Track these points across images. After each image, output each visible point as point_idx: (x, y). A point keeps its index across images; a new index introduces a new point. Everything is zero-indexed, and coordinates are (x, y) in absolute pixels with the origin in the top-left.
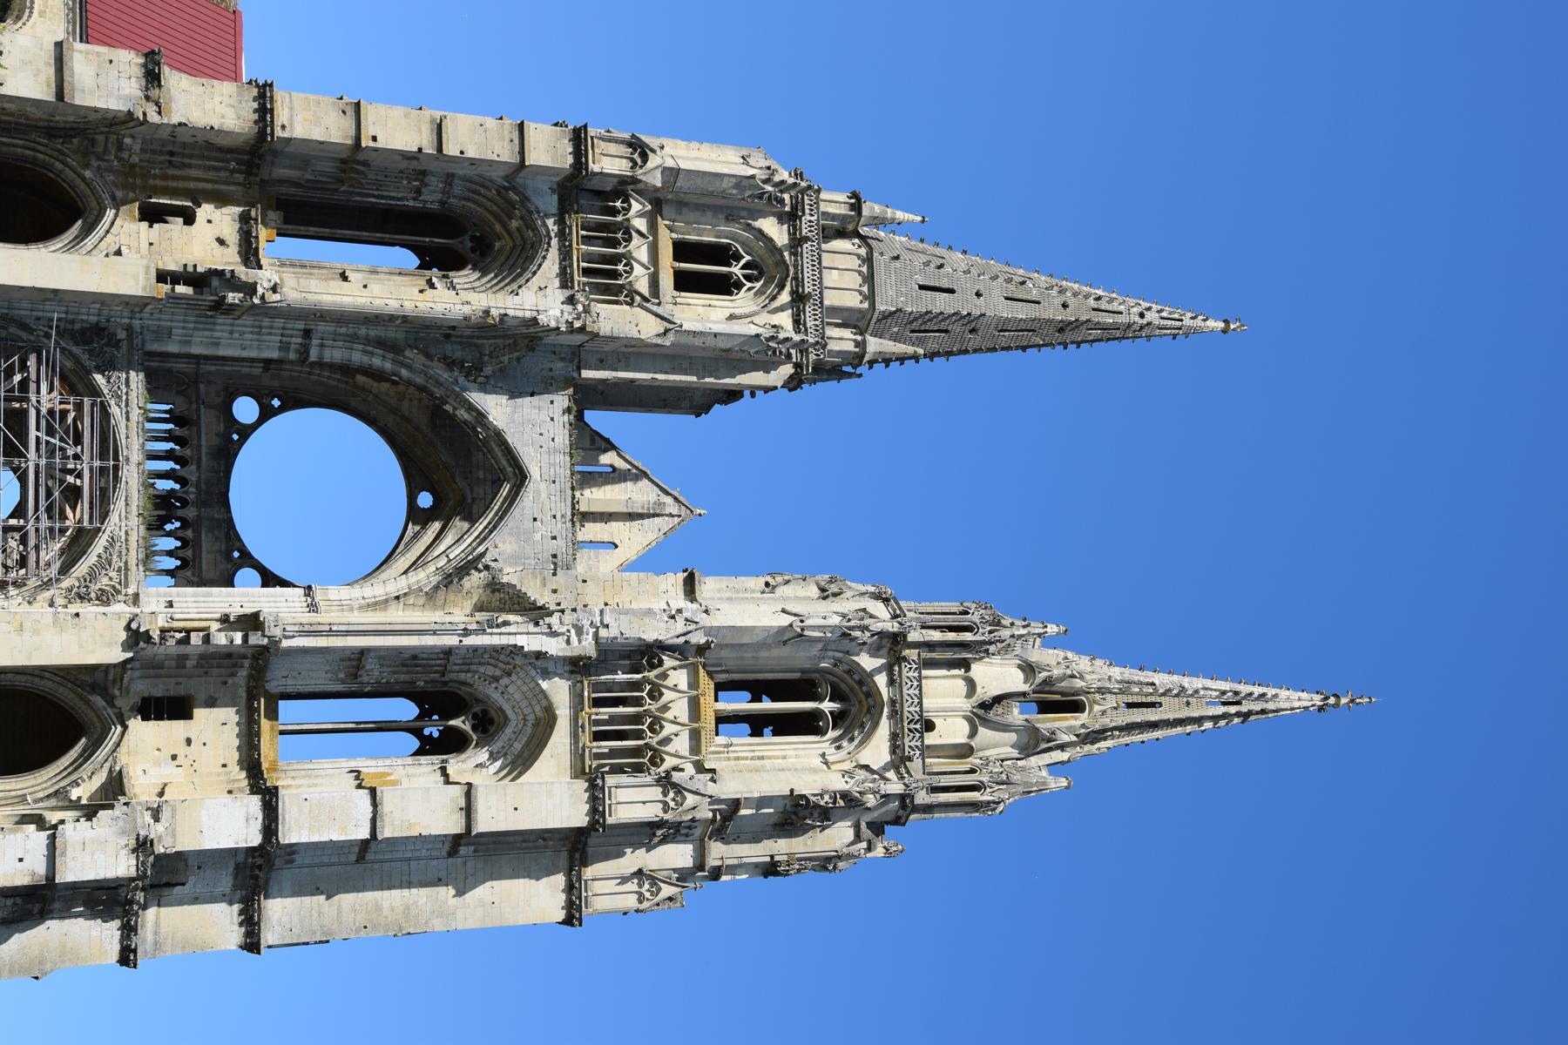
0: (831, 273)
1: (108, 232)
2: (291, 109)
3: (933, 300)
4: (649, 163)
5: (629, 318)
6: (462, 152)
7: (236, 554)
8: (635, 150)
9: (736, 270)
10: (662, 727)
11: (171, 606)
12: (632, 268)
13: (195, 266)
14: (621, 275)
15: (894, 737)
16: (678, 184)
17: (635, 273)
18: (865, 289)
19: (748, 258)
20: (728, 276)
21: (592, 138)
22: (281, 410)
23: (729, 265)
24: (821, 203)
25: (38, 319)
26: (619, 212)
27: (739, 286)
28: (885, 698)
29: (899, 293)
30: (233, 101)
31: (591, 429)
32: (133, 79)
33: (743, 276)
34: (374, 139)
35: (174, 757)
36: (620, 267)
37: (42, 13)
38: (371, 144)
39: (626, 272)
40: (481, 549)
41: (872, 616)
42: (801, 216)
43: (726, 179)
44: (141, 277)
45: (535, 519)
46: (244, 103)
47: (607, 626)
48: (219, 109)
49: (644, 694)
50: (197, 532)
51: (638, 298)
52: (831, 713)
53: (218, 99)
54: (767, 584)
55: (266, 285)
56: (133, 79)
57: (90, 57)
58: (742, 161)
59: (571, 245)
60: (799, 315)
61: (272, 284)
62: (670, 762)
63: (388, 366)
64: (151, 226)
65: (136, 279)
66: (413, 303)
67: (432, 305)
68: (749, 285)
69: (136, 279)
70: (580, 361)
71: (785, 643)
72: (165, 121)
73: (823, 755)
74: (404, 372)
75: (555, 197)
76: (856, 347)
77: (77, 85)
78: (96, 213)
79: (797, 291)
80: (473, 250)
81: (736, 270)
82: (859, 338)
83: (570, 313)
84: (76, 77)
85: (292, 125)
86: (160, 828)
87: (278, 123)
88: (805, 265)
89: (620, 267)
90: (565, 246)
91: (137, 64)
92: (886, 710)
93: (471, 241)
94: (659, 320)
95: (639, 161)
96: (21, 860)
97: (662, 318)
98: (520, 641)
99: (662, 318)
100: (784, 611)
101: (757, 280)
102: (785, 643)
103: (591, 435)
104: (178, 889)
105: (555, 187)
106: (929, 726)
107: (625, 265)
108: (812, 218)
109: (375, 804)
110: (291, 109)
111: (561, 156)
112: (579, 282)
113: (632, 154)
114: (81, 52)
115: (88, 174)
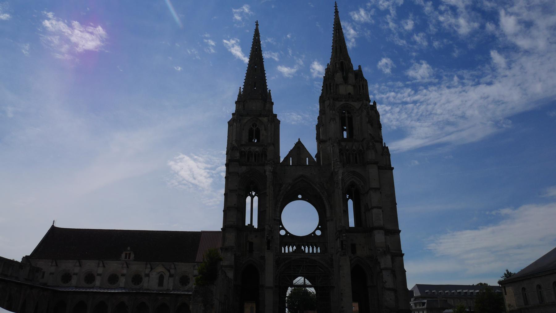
7: (313, 235)
9: (254, 129)
10: (354, 149)
11: (333, 248)
15: (353, 101)
22: (282, 225)
25: (275, 273)
27: (258, 128)
28: (345, 102)
34: (235, 204)
35: (363, 247)
36: (257, 153)
40: (318, 185)
41: (330, 104)
45: (311, 174)
47: (336, 159)
49: (347, 153)
51: (264, 150)
52: (348, 114)
54: (322, 126)
58: (231, 126)
62: (361, 148)
63: (280, 203)
71: (336, 123)
73: (357, 116)
74: (281, 200)
75: (243, 167)
81: (254, 129)
82: (268, 103)
86: (381, 250)
89: (257, 153)
92: (347, 102)
96: (388, 276)
98: (340, 177)
100: (329, 123)
102: (336, 123)
104: (389, 246)
106: (349, 94)
107: (256, 152)
109: (375, 207)
115: (244, 263)
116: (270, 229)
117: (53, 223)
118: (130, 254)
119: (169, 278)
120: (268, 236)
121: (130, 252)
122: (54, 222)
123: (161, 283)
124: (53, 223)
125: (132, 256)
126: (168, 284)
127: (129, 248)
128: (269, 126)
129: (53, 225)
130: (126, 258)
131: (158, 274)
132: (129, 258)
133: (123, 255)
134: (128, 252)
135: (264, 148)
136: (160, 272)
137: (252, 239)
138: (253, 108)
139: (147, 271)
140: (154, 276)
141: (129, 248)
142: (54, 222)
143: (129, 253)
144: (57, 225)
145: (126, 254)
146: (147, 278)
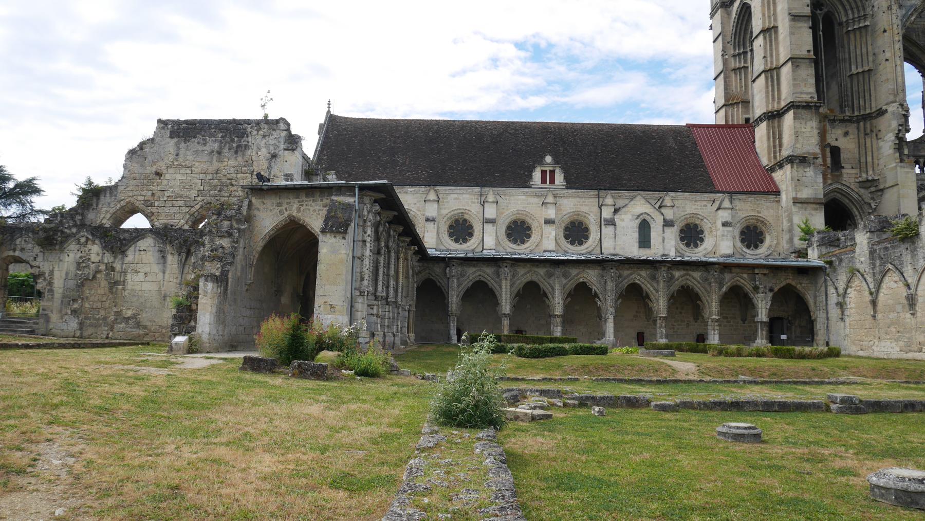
1: (849, 187)
2: (801, 93)
6: (808, 6)
13: (895, 144)
30: (803, 122)
32: (805, 170)
34: (809, 51)
37: (759, 212)
38: (812, 53)
44: (906, 170)
46: (804, 117)
48: (809, 129)
50: (921, 156)
53: (803, 130)
55: (900, 110)
56: (805, 170)
57: (798, 189)
61: (900, 107)
64: (843, 167)
65: (908, 173)
66: (895, 36)
67: (895, 26)
69: (908, 173)
72: (820, 156)
77: (813, 196)
78: (835, 193)
80: (821, 10)
84: (810, 197)
85: (807, 93)
87: (810, 100)
91: (797, 168)
93: (816, 10)
110: (801, 93)
114: (796, 194)
116: (904, 113)
117: (329, 107)
118: (552, 173)
119: (663, 228)
120: (900, 128)
121: (551, 169)
122: (329, 104)
123: (644, 240)
124: (329, 107)
125: (559, 178)
126: (663, 241)
127: (548, 159)
129: (329, 112)
130: (544, 181)
131: (637, 218)
132: (552, 181)
133: (537, 176)
134: (548, 169)
136: (642, 214)
137: (837, 140)
139: (607, 213)
140: (627, 223)
141: (548, 159)
142: (329, 104)
143: (550, 171)
144: (337, 111)
145: (544, 173)
146: (611, 228)
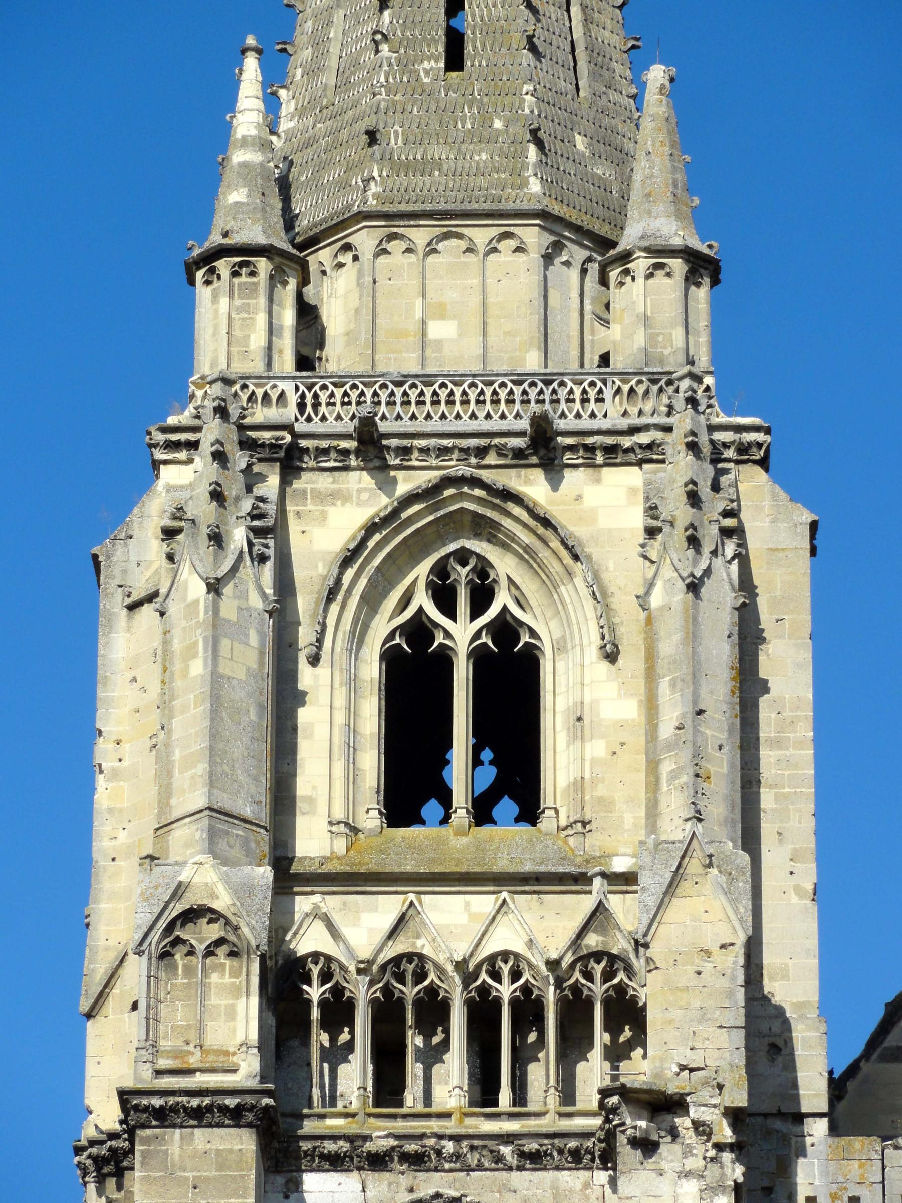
0: (439, 343)
3: (488, 28)
4: (216, 905)
5: (685, 976)
8: (178, 941)
12: (505, 955)
14: (526, 990)
16: (247, 812)
17: (518, 946)
18: (481, 235)
19: (423, 600)
20: (479, 656)
21: (159, 1073)
23: (445, 658)
24: (239, 368)
26: (338, 991)
29: (485, 138)
31: (867, 1054)
33: (474, 616)
36: (506, 991)
39: (516, 975)
42: (296, 436)
43: (224, 668)
51: (593, 941)
59: (457, 1138)
60: (590, 449)
68: (502, 599)
70: (780, 1115)
76: (698, 285)
79: (519, 453)
82: (641, 264)
83: (688, 1152)
88: (435, 425)
89: (506, 991)
90: (457, 1156)
94: (685, 887)
95: (214, 932)
97: (678, 876)
99: (678, 876)
101: (483, 569)
103: (884, 1058)
105: (280, 1180)
107: (496, 976)
108: (293, 399)
111: (220, 1168)
112: (561, 1115)
113: (191, 953)
128: (656, 599)
135: (600, 909)
138: (437, 330)
